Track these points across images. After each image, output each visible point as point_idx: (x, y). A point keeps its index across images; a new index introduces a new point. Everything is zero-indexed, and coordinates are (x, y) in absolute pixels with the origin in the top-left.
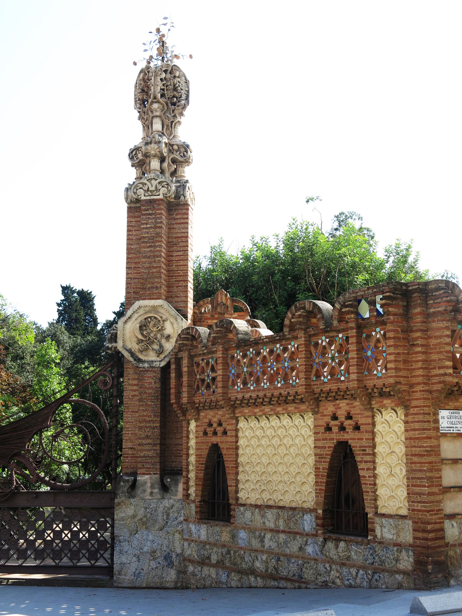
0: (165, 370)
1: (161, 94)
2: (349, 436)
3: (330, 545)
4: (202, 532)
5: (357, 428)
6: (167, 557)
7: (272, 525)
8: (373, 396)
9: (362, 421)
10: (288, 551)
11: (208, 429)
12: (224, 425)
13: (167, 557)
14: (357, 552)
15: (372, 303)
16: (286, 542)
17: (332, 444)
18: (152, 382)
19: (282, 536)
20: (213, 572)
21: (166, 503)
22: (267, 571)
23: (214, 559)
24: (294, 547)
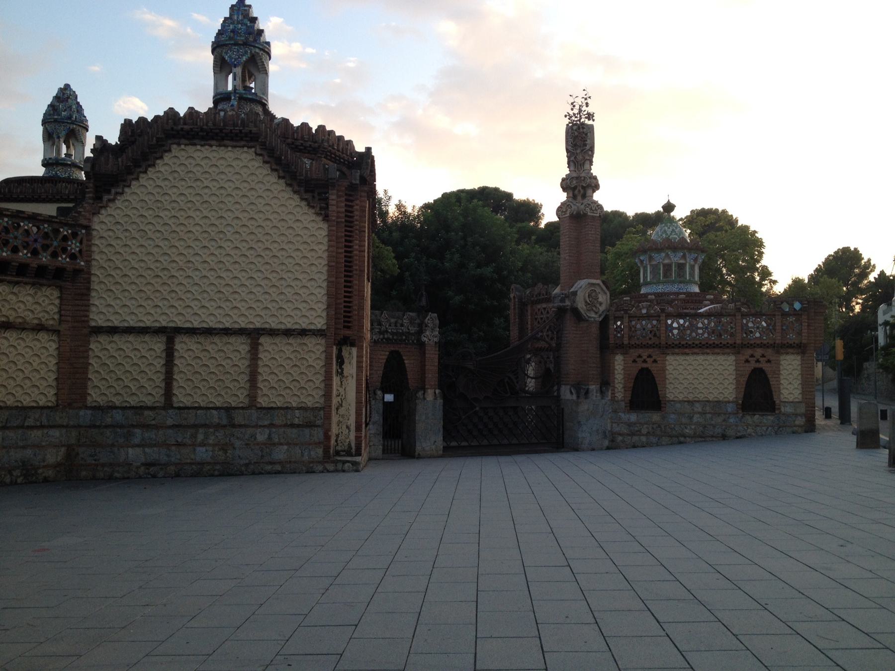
0: (604, 324)
1: (580, 141)
2: (763, 365)
3: (748, 417)
4: (633, 417)
5: (769, 361)
6: (604, 432)
7: (700, 410)
8: (783, 348)
9: (772, 358)
10: (713, 422)
11: (637, 359)
12: (654, 357)
13: (604, 432)
14: (770, 418)
15: (791, 305)
16: (711, 419)
17: (750, 369)
18: (595, 330)
19: (708, 416)
20: (644, 439)
21: (603, 401)
22: (695, 433)
23: (644, 431)
24: (719, 420)
